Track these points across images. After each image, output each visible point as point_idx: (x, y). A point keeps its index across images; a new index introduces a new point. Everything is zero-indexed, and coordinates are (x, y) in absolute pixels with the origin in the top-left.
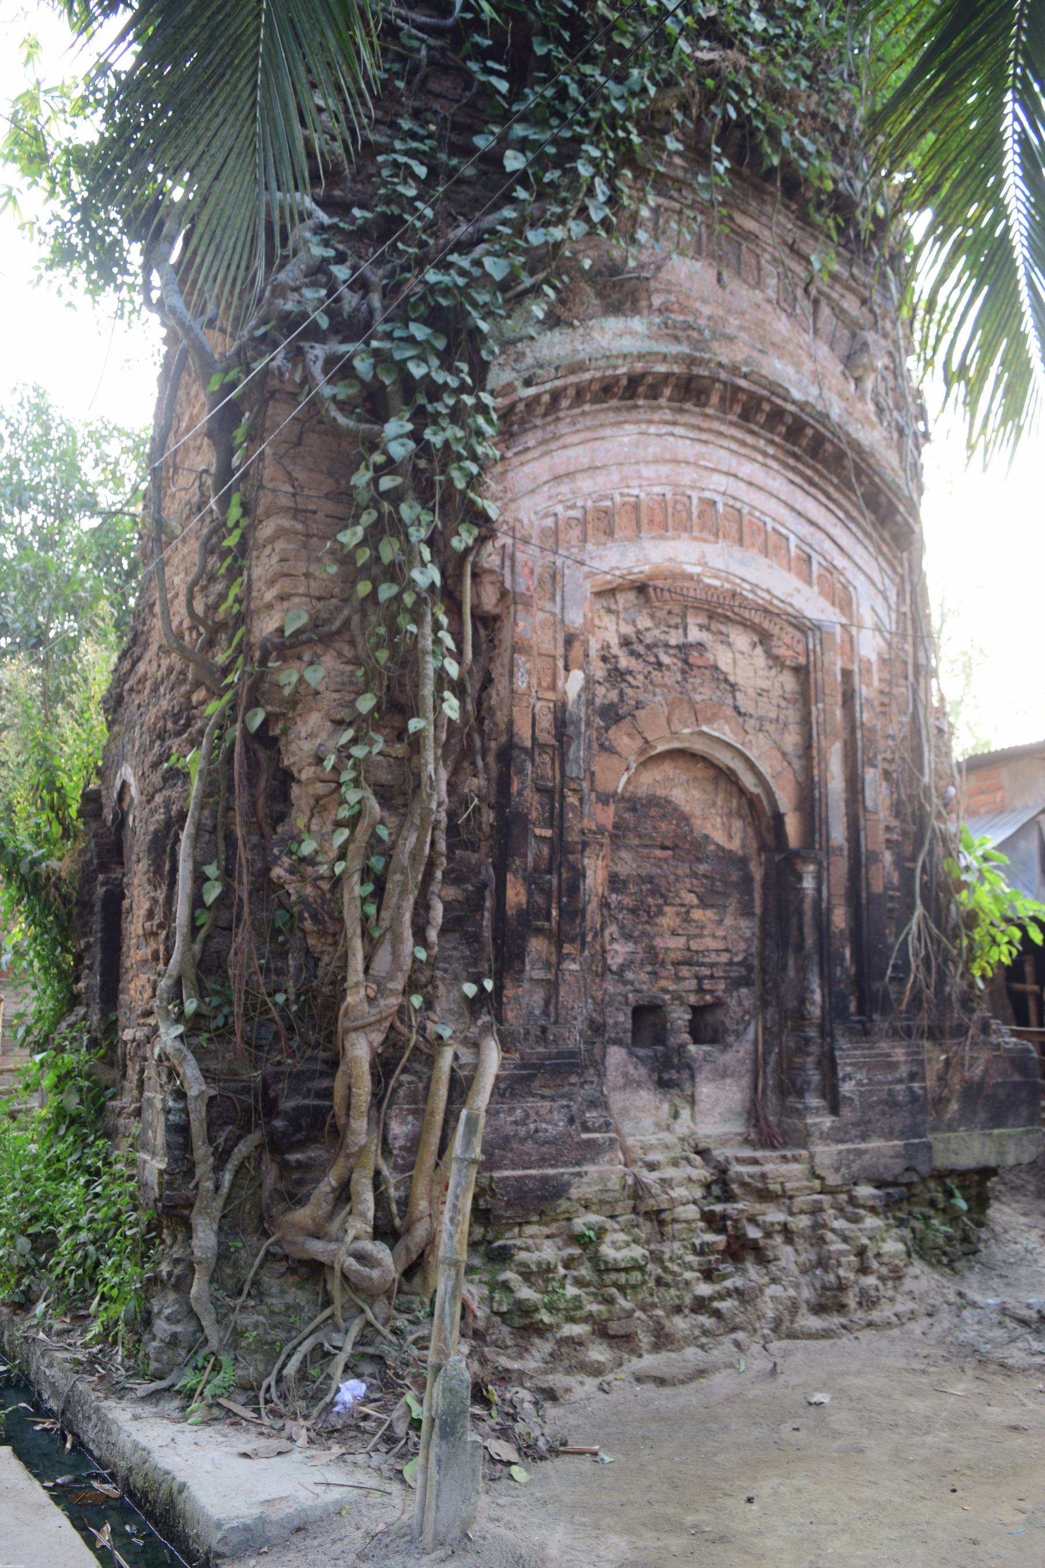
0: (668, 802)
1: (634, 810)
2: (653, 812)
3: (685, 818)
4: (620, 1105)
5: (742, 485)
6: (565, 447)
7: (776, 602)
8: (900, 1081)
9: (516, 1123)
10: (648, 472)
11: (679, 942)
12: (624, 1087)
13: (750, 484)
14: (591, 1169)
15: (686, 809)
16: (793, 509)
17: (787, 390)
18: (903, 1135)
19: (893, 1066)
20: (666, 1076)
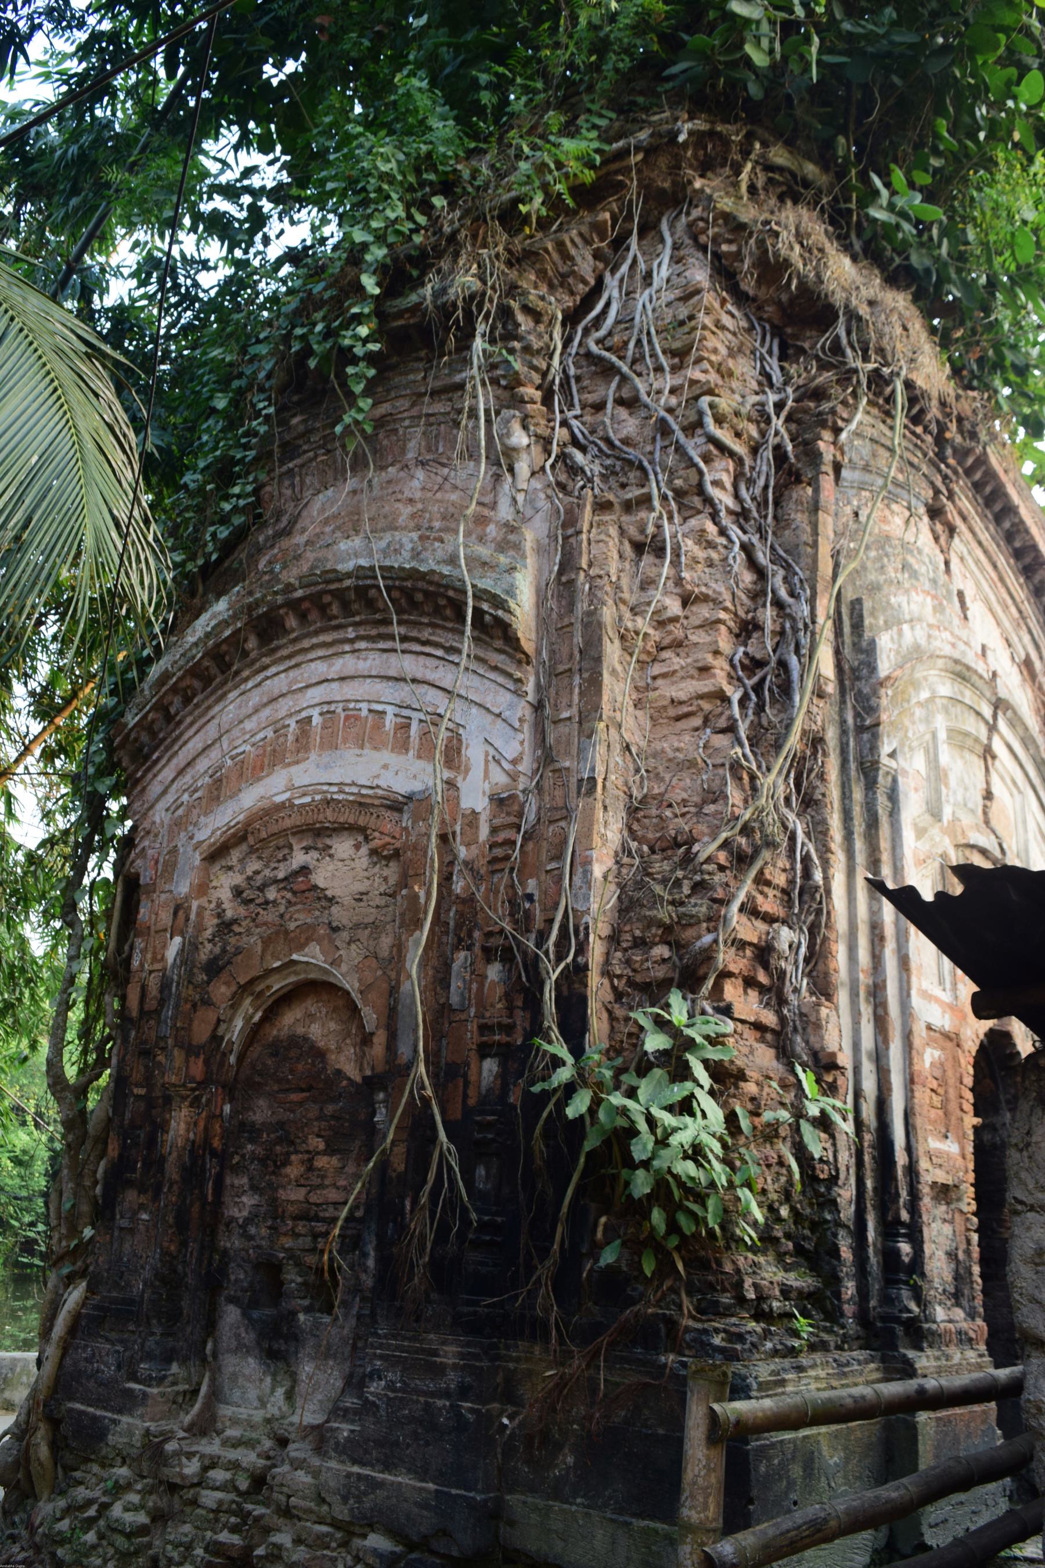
0: (306, 1039)
1: (275, 1054)
2: (293, 1053)
3: (320, 1054)
4: (231, 1369)
5: (335, 685)
6: (186, 743)
7: (364, 791)
8: (446, 1394)
9: (86, 1360)
10: (249, 725)
11: (299, 1194)
12: (235, 1351)
13: (342, 679)
14: (125, 1419)
15: (321, 1044)
16: (389, 678)
17: (335, 571)
18: (439, 1477)
19: (439, 1370)
20: (276, 1346)
